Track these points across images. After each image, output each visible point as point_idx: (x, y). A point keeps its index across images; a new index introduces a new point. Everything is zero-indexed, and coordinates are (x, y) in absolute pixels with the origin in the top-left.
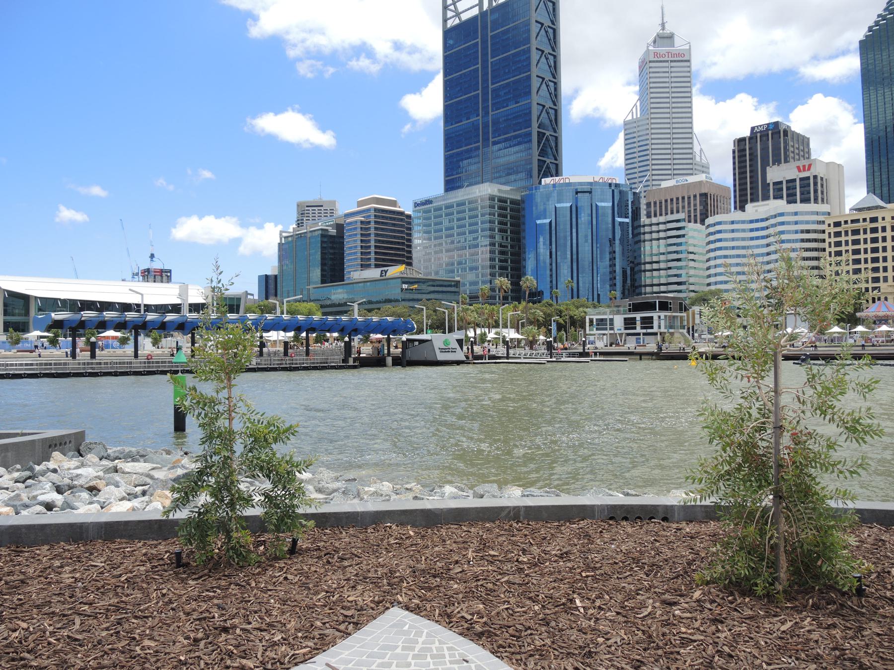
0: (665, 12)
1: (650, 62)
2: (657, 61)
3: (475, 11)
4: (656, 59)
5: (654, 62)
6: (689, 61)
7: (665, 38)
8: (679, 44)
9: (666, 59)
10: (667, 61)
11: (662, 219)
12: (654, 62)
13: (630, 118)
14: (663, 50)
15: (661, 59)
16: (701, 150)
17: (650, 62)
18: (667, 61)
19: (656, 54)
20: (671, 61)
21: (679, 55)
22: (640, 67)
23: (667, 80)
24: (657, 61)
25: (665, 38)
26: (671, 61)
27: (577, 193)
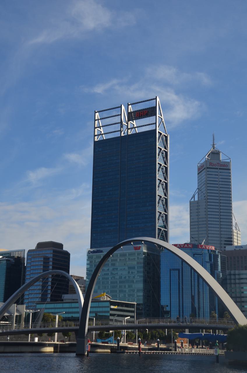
0: (215, 138)
1: (207, 168)
2: (211, 168)
3: (117, 135)
4: (211, 167)
5: (209, 168)
6: (229, 169)
7: (215, 154)
8: (222, 157)
9: (217, 167)
10: (217, 169)
11: (237, 272)
12: (209, 168)
13: (193, 200)
14: (215, 162)
15: (214, 167)
16: (236, 223)
17: (207, 168)
18: (217, 169)
19: (211, 164)
20: (220, 169)
21: (224, 165)
22: (199, 169)
23: (217, 180)
24: (211, 168)
25: (215, 154)
26: (220, 169)
27: (194, 255)
